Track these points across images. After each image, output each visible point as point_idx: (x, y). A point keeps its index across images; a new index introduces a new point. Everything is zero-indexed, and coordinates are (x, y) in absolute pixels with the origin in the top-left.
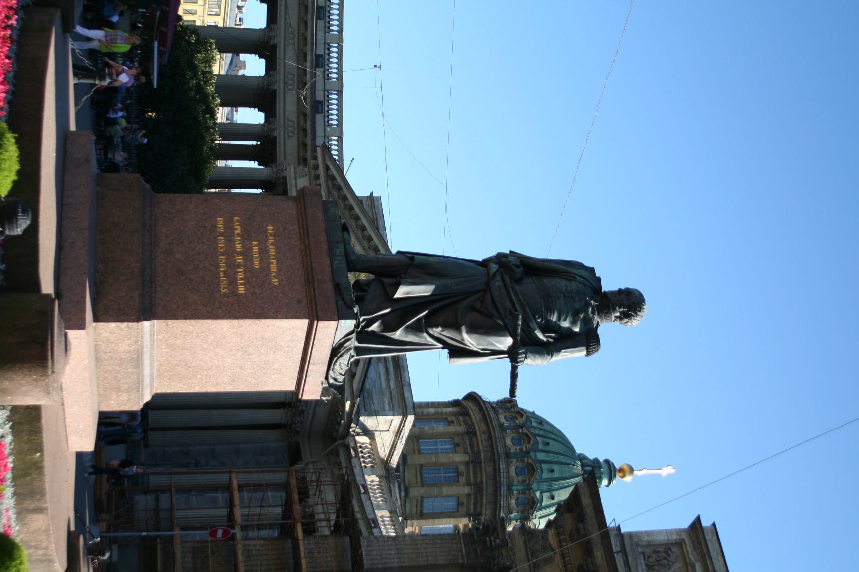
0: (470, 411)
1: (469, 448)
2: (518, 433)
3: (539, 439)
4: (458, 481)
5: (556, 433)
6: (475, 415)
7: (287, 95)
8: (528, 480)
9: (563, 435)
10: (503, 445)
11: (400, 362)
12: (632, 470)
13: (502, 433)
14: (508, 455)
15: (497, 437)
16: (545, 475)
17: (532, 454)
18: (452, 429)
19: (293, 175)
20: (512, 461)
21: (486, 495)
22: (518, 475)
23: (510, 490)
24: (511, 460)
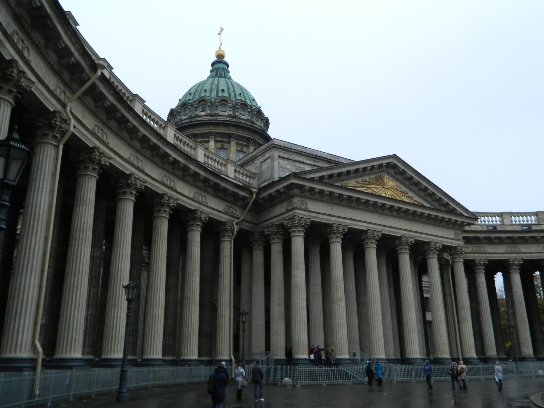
0: (215, 131)
1: (244, 143)
2: (238, 109)
3: (238, 98)
7: (178, 190)
19: (307, 213)
22: (258, 122)
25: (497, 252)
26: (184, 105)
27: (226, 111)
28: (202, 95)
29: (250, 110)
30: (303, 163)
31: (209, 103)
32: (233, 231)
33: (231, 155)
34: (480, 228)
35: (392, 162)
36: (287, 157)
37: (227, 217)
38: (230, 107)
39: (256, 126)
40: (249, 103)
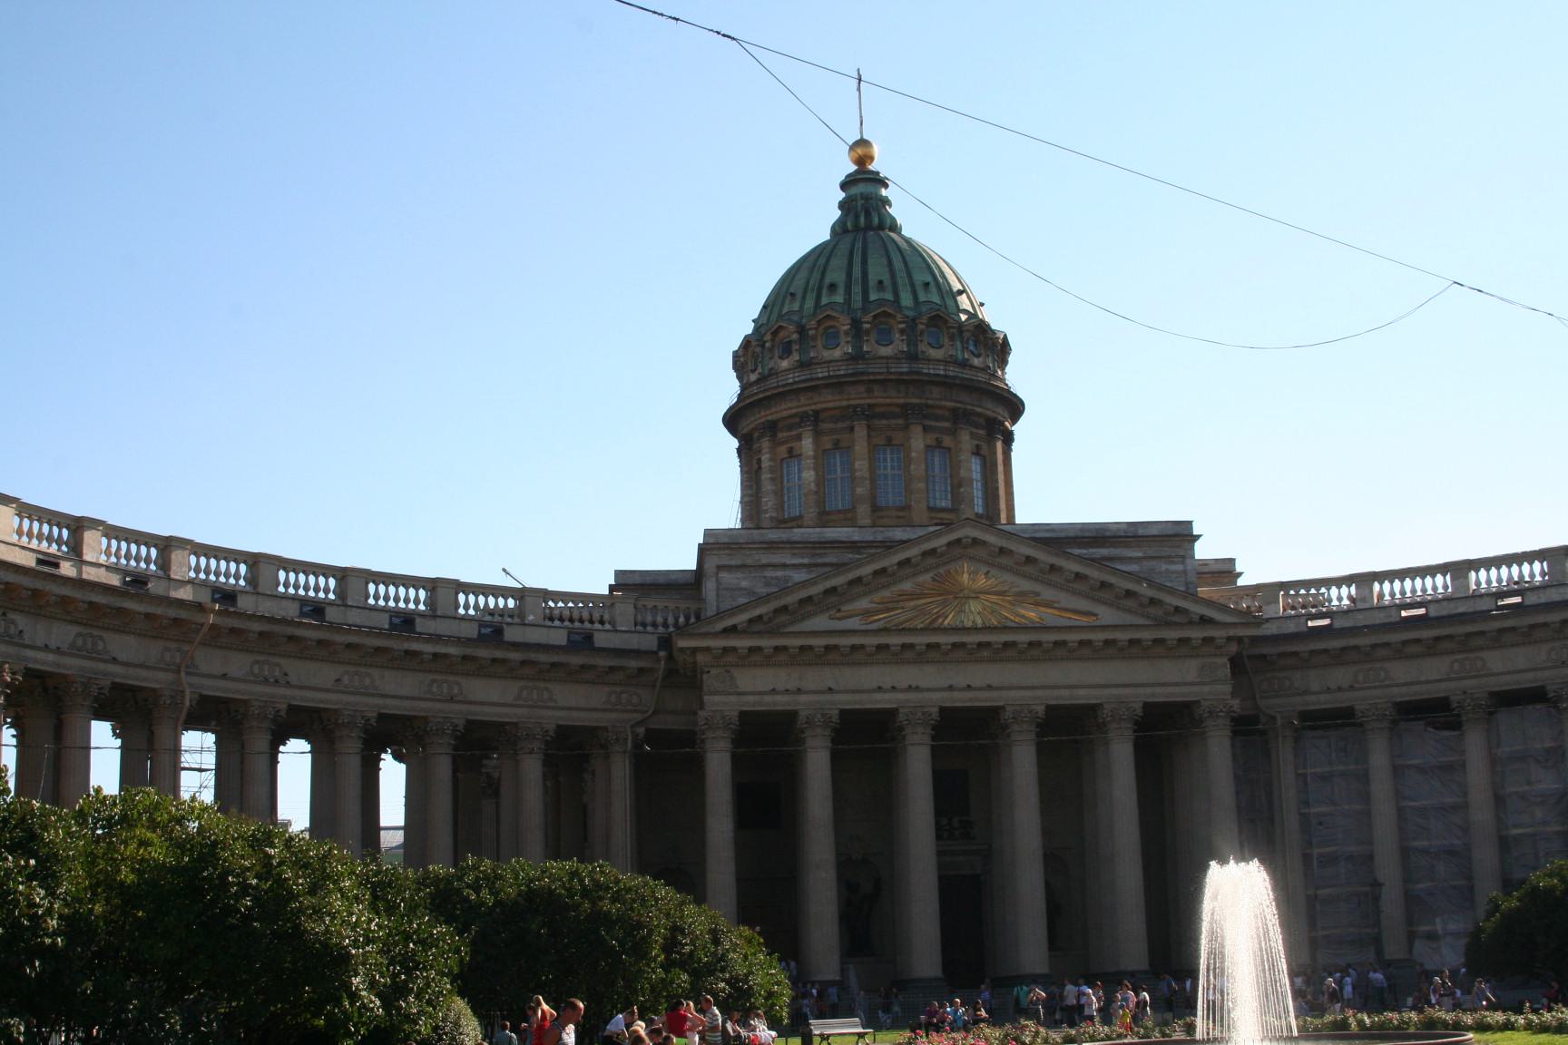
0: (813, 407)
1: (893, 422)
2: (868, 332)
4: (949, 449)
5: (839, 262)
6: (829, 401)
8: (952, 330)
9: (820, 245)
10: (895, 361)
11: (1087, 534)
12: (863, 143)
13: (868, 359)
14: (913, 357)
15: (885, 370)
16: (936, 299)
17: (911, 314)
18: (861, 447)
19: (733, 698)
20: (923, 352)
21: (973, 405)
22: (941, 347)
23: (964, 364)
24: (919, 353)
25: (1423, 679)
26: (747, 343)
27: (837, 346)
28: (785, 310)
29: (903, 326)
30: (784, 566)
31: (795, 332)
32: (626, 739)
33: (857, 465)
34: (1379, 618)
35: (967, 537)
36: (739, 563)
37: (614, 716)
38: (846, 333)
39: (927, 369)
40: (906, 300)
